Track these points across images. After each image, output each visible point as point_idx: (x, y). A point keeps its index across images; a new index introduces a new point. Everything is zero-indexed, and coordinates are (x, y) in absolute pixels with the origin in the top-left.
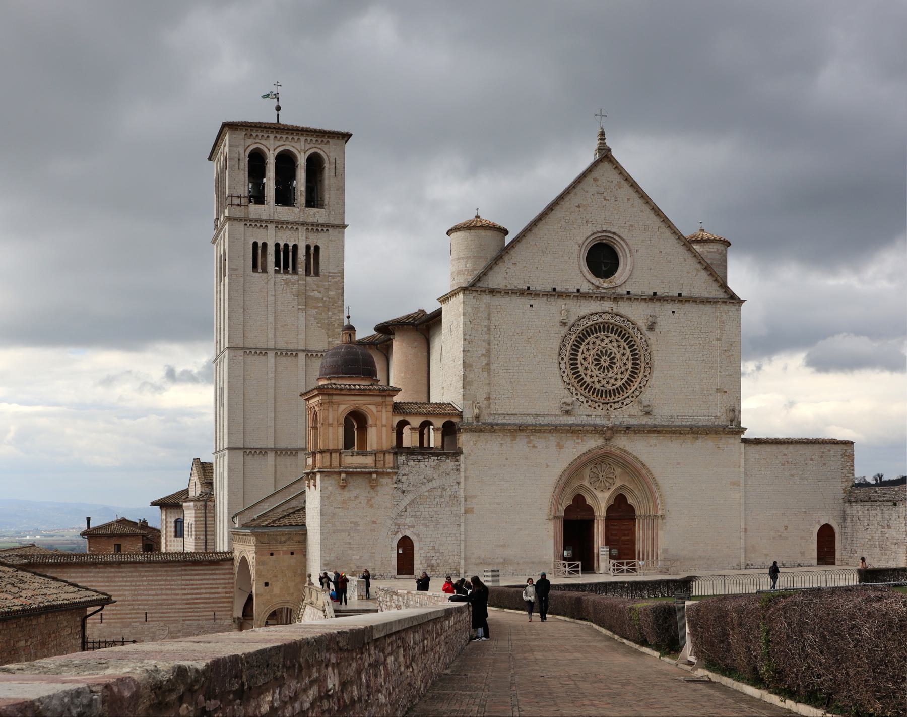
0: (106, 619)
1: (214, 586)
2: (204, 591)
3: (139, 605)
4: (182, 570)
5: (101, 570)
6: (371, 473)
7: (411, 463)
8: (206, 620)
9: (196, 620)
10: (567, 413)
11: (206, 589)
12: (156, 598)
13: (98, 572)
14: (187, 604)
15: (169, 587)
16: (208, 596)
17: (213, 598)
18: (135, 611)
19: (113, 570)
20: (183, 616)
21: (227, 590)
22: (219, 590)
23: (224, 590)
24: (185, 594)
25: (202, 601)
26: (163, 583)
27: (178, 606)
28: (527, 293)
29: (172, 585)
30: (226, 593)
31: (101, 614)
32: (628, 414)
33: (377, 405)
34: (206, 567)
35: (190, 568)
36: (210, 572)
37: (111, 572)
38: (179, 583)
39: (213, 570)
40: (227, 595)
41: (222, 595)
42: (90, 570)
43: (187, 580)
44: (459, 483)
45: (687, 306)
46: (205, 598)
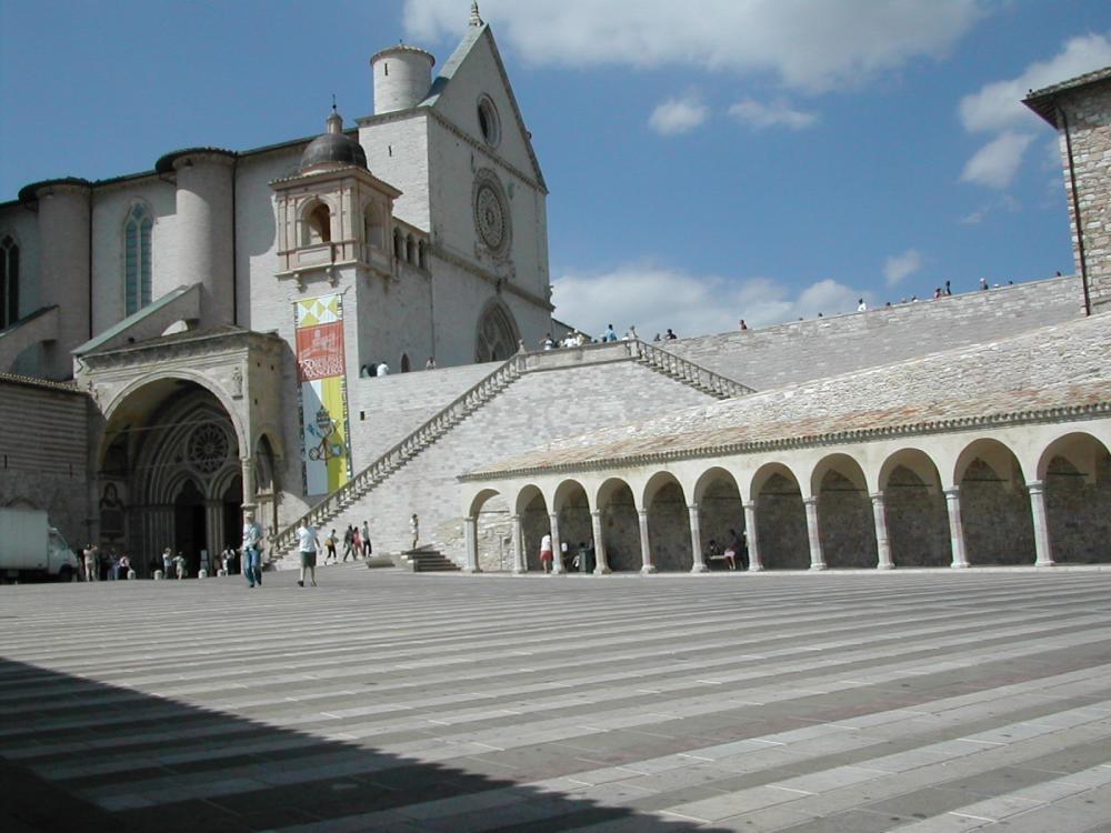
1: (71, 429)
2: (60, 434)
4: (40, 403)
6: (386, 278)
8: (64, 473)
9: (52, 472)
10: (479, 258)
11: (63, 431)
12: (15, 435)
15: (27, 423)
16: (63, 441)
20: (41, 466)
22: (75, 436)
23: (79, 436)
26: (21, 416)
28: (456, 131)
29: (30, 421)
30: (81, 440)
32: (503, 272)
33: (384, 204)
34: (63, 403)
35: (46, 400)
38: (38, 418)
40: (81, 443)
43: (46, 417)
44: (432, 307)
45: (524, 185)
46: (62, 444)
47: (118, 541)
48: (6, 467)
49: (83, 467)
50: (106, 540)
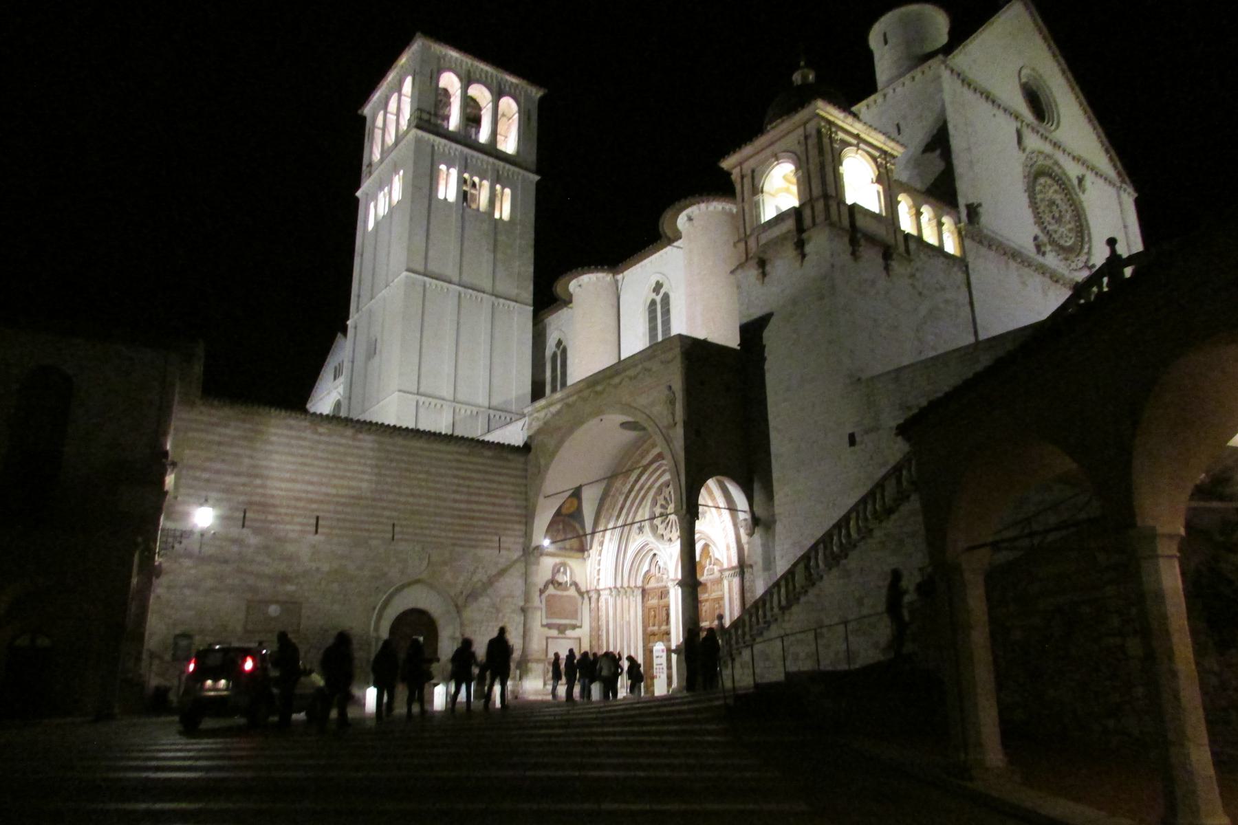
0: (323, 526)
3: (384, 508)
5: (323, 438)
7: (922, 255)
13: (319, 442)
14: (460, 517)
16: (490, 508)
17: (498, 513)
18: (375, 520)
19: (343, 441)
21: (519, 503)
22: (508, 502)
24: (455, 501)
25: (482, 515)
27: (444, 520)
30: (517, 507)
31: (317, 518)
36: (494, 470)
37: (340, 445)
39: (500, 467)
40: (518, 511)
41: (512, 510)
42: (303, 435)
45: (1101, 182)
46: (487, 512)
47: (569, 633)
48: (393, 539)
49: (521, 540)
50: (554, 633)
